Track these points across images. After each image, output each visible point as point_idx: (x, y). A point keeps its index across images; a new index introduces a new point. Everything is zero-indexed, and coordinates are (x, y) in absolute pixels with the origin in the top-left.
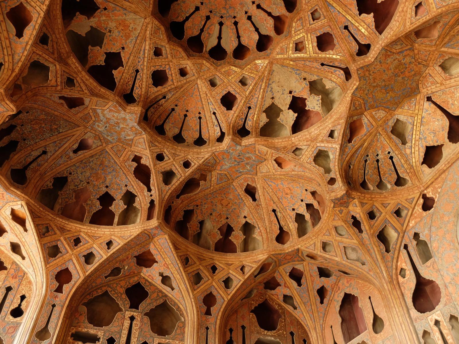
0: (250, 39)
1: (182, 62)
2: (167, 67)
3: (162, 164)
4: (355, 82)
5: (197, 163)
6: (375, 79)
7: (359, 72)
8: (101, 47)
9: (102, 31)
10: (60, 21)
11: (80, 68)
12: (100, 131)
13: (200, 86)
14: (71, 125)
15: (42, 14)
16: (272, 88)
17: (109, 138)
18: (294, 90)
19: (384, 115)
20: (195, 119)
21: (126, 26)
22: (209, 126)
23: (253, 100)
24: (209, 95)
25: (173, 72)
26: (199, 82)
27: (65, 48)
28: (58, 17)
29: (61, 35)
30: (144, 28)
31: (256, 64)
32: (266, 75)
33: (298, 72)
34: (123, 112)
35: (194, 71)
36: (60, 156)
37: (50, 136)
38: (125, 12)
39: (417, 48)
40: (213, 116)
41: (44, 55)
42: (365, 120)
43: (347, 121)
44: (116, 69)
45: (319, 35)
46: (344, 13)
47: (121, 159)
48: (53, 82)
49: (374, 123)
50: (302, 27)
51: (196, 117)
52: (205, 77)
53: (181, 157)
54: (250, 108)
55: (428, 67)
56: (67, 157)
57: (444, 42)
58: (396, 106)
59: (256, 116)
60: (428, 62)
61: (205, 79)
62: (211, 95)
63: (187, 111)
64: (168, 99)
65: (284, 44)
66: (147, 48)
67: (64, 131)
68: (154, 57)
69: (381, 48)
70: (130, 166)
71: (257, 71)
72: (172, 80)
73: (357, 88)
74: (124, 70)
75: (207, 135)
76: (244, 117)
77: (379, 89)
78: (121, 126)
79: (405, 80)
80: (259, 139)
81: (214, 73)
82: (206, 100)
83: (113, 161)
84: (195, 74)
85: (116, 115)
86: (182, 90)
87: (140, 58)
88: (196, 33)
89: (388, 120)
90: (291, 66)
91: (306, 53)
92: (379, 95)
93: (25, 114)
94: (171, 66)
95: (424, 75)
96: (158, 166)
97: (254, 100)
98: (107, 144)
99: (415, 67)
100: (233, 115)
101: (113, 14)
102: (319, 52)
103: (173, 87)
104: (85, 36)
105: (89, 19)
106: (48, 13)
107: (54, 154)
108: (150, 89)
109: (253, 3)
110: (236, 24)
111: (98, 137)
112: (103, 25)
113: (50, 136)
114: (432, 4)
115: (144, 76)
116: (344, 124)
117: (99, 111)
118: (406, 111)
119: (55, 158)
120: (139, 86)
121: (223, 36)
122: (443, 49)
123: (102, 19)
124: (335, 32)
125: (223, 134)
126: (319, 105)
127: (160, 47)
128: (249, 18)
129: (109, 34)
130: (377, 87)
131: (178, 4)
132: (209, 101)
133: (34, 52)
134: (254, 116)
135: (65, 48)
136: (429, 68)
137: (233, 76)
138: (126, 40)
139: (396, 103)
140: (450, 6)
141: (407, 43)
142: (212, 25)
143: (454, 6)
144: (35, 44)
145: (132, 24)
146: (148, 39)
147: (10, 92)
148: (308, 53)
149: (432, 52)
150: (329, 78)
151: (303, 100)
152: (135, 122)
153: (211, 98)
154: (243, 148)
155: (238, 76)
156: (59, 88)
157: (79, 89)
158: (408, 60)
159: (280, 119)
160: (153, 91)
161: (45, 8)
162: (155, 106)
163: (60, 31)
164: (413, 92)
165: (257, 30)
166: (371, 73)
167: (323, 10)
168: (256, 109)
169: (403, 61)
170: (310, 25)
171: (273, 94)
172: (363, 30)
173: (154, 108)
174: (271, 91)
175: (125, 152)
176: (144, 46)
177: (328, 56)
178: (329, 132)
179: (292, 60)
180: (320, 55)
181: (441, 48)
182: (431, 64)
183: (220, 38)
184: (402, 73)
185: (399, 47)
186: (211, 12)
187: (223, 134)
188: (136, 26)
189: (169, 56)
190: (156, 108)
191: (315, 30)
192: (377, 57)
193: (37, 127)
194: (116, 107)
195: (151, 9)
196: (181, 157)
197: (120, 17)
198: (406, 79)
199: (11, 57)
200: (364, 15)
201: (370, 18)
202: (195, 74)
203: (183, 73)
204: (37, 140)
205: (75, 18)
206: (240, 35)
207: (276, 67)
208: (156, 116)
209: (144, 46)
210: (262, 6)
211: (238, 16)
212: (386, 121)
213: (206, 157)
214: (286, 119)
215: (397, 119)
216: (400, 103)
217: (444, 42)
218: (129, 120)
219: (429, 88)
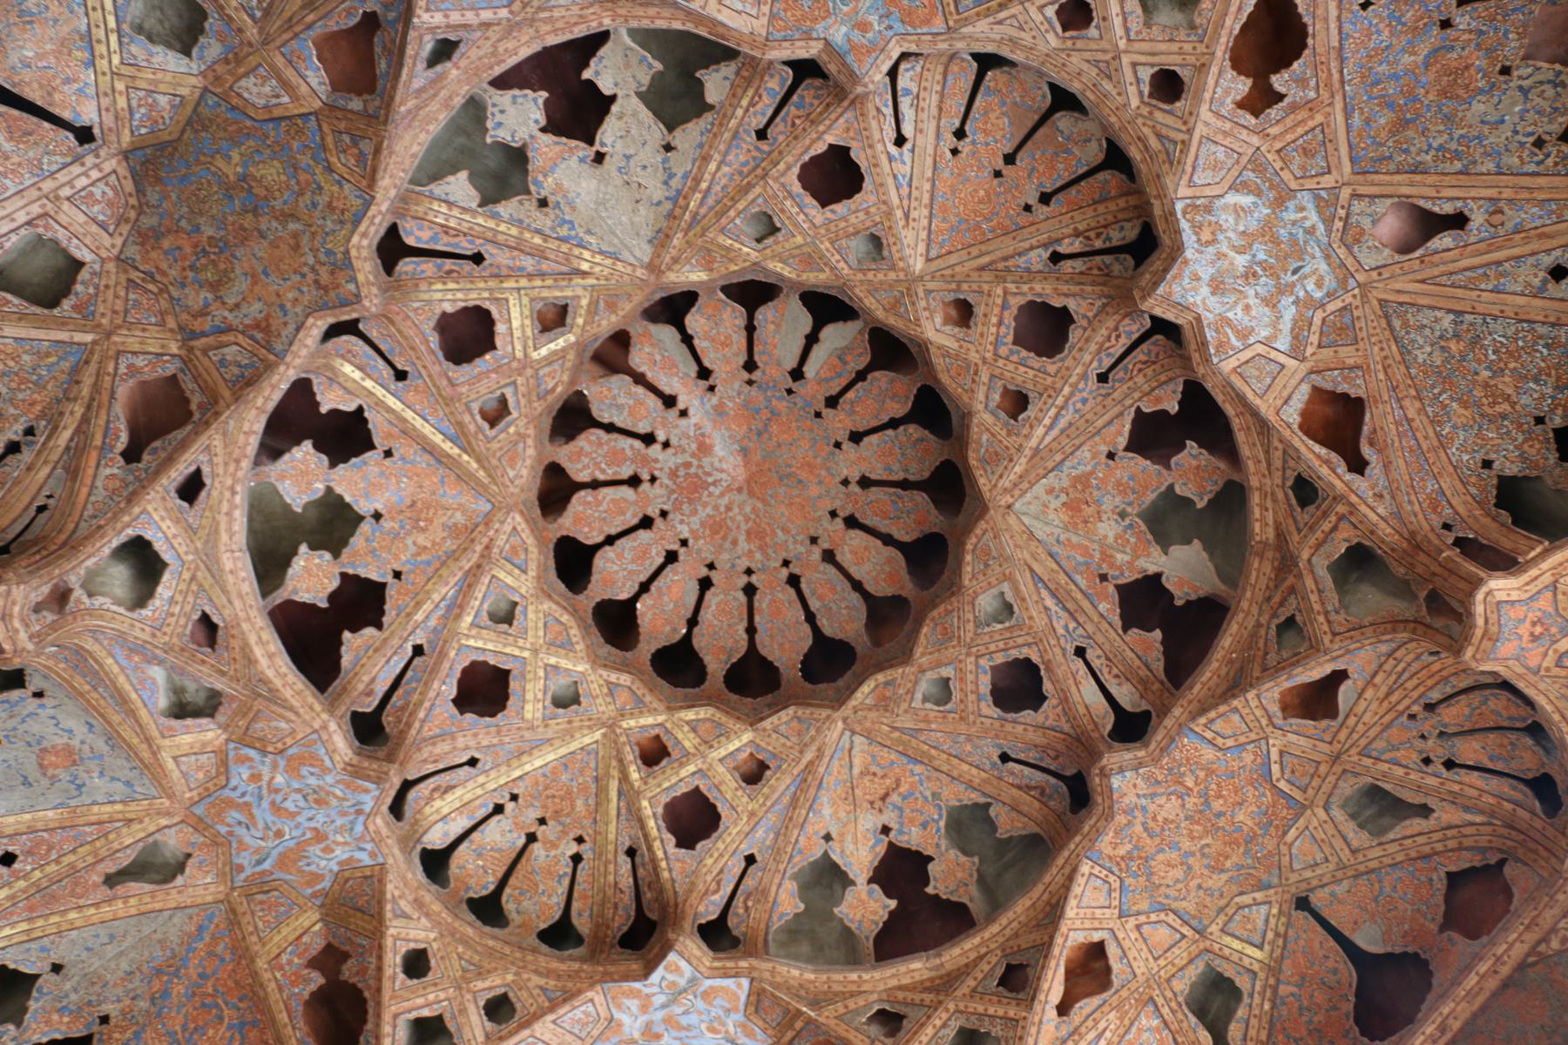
0: (715, 325)
1: (952, 344)
2: (1003, 351)
3: (1172, 61)
4: (365, 242)
5: (1033, 11)
6: (296, 247)
7: (351, 287)
8: (1171, 487)
9: (1144, 527)
10: (1228, 641)
11: (1255, 498)
12: (1327, 257)
13: (921, 248)
14: (1405, 324)
15: (1251, 695)
16: (666, 183)
17: (1313, 218)
18: (585, 166)
19: (243, 83)
20: (980, 137)
21: (1072, 507)
22: (935, 98)
23: (742, 158)
24: (899, 213)
25: (993, 330)
26: (918, 265)
27: (1258, 570)
28: (1222, 653)
29: (1245, 605)
30: (1025, 485)
31: (711, 270)
32: (680, 235)
33: (563, 232)
34: (1208, 317)
35: (923, 304)
36: (1517, 237)
37: (1495, 318)
38: (1055, 549)
39: (169, 335)
40: (907, 130)
41: (1317, 607)
42: (315, 80)
43: (388, 104)
44: (1164, 412)
45: (487, 357)
46: (409, 414)
47: (1319, 118)
48: (1345, 535)
49: (280, 61)
50: (541, 373)
51: (973, 143)
52: (892, 275)
53: (1087, 55)
54: (761, 134)
55: (118, 258)
56: (1497, 219)
57: (93, 367)
58: (205, 112)
59: (745, 102)
60: (123, 278)
61: (893, 268)
62: (889, 214)
63: (998, 174)
64: (1045, 246)
65: (604, 323)
66: (1040, 431)
67: (1439, 314)
68: (1031, 395)
69: (288, 359)
70: (1302, 82)
71: (709, 250)
72: (1004, 306)
73: (357, 222)
74: (1140, 399)
75: (954, 68)
76: (790, 109)
77: (278, 204)
78: (1241, 261)
79: (189, 221)
80: (745, 49)
81: (860, 276)
82: (915, 193)
83: (1357, 120)
84: (921, 294)
85: (1236, 315)
86: (986, 259)
87: (1077, 411)
88: (881, 378)
89: (227, 62)
90: (587, 254)
91: (532, 300)
92: (271, 172)
93: (1496, 465)
94: (990, 348)
95: (125, 229)
96: (1191, 59)
97: (738, 157)
98: (1334, 190)
99: (164, 266)
100: (830, 127)
101: (1092, 557)
102: (487, 305)
103: (1012, 287)
104: (1196, 541)
105: (1158, 576)
106: (1235, 685)
107: (1533, 254)
108: (1090, 314)
109: (684, 413)
110: (750, 366)
111: (1352, 236)
112: (1133, 540)
113: (1495, 318)
114: (163, 519)
115: (1087, 358)
116: (398, 99)
117: (1283, 343)
118: (162, 88)
119: (1541, 236)
120: (1118, 336)
121: (800, 343)
122: (89, 338)
123: (1127, 558)
124: (437, 368)
125: (893, 74)
126: (496, 110)
127: (1002, 415)
128: (704, 373)
129: (1129, 510)
130: (283, 214)
131: (906, 471)
132: (905, 191)
133: (1334, 634)
134: (752, 104)
135: (1259, 571)
136: (115, 252)
137: (797, 252)
138: (1092, 473)
139: (205, 128)
140: (110, 532)
141: (206, 361)
142: (827, 380)
143: (102, 537)
144: (1315, 648)
145: (1052, 506)
146: (1028, 452)
147: (1456, 628)
148: (525, 300)
149: (119, 321)
150: (456, 212)
151: (555, 126)
152: (1186, 262)
153: (896, 201)
154: (820, 27)
155: (778, 249)
156: (1341, 509)
157: (1292, 463)
158: (198, 298)
159: (650, 66)
160: (1084, 304)
161: (1235, 703)
162: (1098, 244)
163: (1241, 615)
164: (152, 161)
165: (687, 340)
166: (310, 277)
167: (472, 428)
168: (740, 124)
169: (210, 296)
170: (514, 383)
171: (663, 162)
172: (348, 369)
173: (1109, 239)
174: (672, 176)
175: (1289, 137)
176: (1048, 439)
177: (460, 295)
178: (456, 56)
179: (584, 274)
180: (486, 295)
181: (95, 342)
182: (111, 266)
183: (812, 339)
184: (204, 250)
185: (230, 352)
186: (818, 415)
187: (893, 74)
188: (1045, 497)
189: (985, 378)
190: (1098, 235)
191: (495, 371)
192: (298, 329)
193: (1506, 384)
194: (1220, 346)
195: (982, 525)
196: (1087, 55)
197: (1075, 539)
198: (183, 223)
199: (1398, 654)
200: (349, 407)
201: (329, 400)
202: (921, 294)
203: (964, 312)
204: (1542, 330)
205: (1193, 597)
206: (744, 333)
207: (638, 253)
208: (1112, 206)
209: (1048, 439)
210: (659, 403)
211: (737, 385)
212: (235, 58)
213: (982, 26)
214: (628, 66)
215: (187, 52)
216: (189, 123)
217: (93, 367)
218: (1206, 273)
219: (95, 174)
